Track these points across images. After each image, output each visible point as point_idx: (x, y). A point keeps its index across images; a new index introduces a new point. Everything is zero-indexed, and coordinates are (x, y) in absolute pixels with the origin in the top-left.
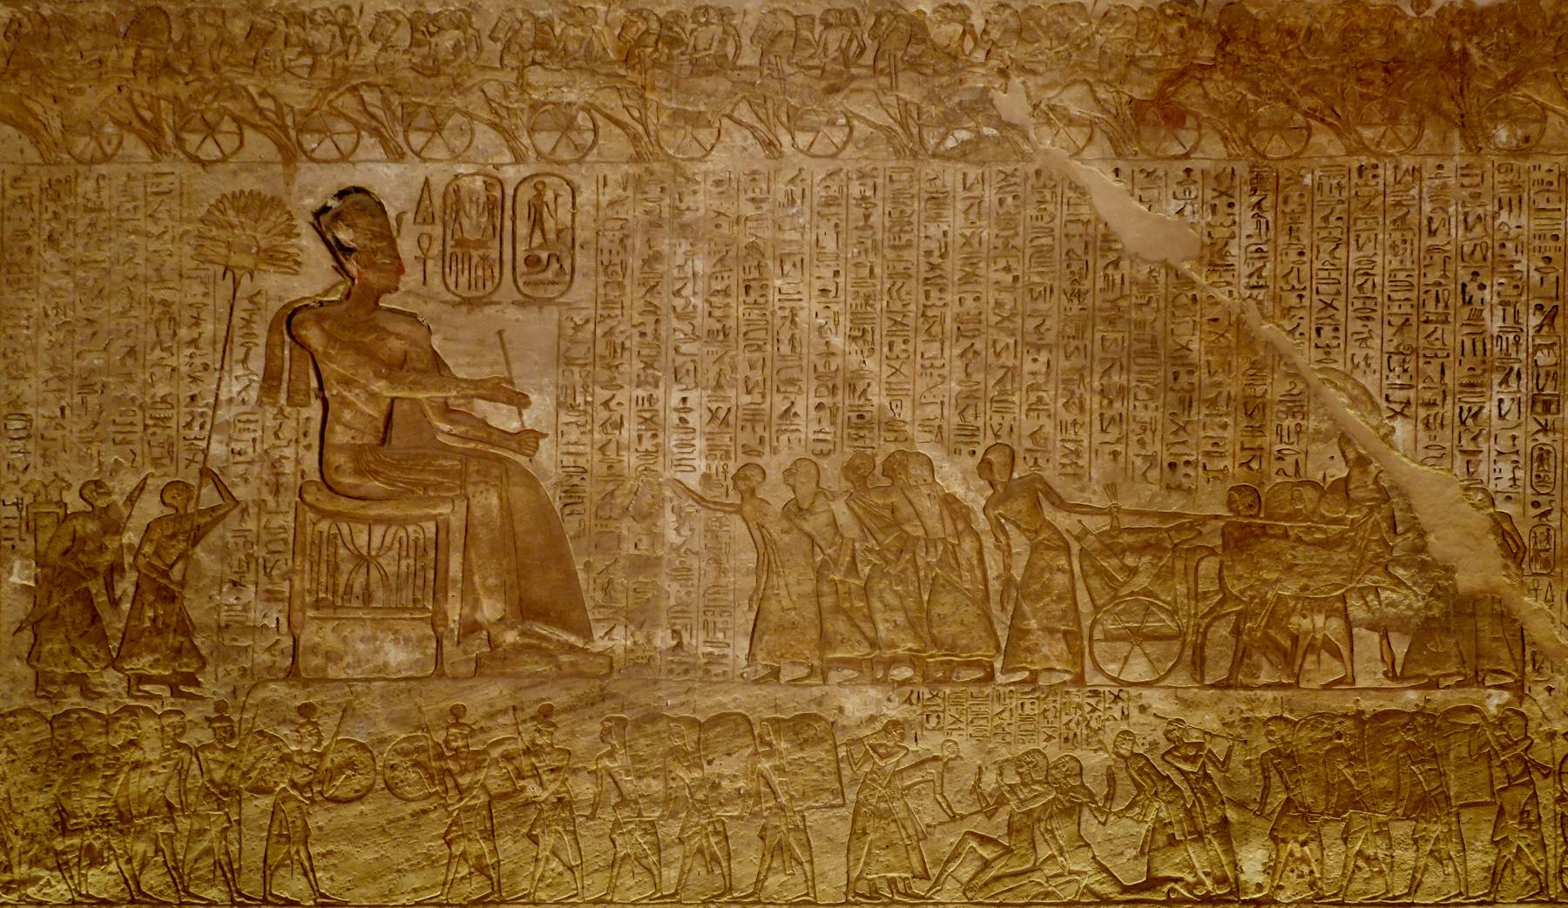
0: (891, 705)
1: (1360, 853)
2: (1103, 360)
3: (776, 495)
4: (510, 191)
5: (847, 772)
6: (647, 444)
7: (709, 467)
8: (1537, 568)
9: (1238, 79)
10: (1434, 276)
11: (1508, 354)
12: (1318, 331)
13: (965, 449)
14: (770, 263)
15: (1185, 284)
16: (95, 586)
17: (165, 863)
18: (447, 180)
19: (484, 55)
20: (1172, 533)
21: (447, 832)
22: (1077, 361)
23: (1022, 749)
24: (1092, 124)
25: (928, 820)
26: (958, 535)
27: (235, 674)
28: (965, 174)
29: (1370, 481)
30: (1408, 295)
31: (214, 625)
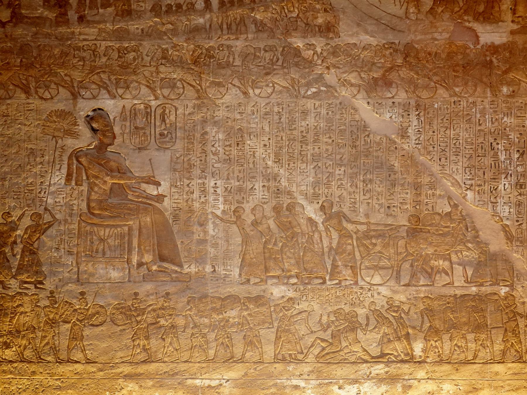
0: (289, 292)
1: (456, 344)
2: (364, 170)
3: (248, 218)
4: (153, 110)
5: (274, 316)
6: (203, 200)
7: (224, 208)
8: (518, 244)
9: (412, 70)
10: (481, 140)
11: (507, 168)
12: (440, 159)
13: (315, 201)
14: (246, 135)
15: (393, 143)
16: (7, 250)
18: (131, 106)
19: (144, 61)
20: (389, 231)
21: (132, 337)
22: (355, 170)
23: (336, 308)
24: (359, 86)
25: (303, 333)
26: (313, 232)
27: (57, 281)
28: (315, 104)
29: (458, 213)
30: (471, 147)
31: (49, 263)
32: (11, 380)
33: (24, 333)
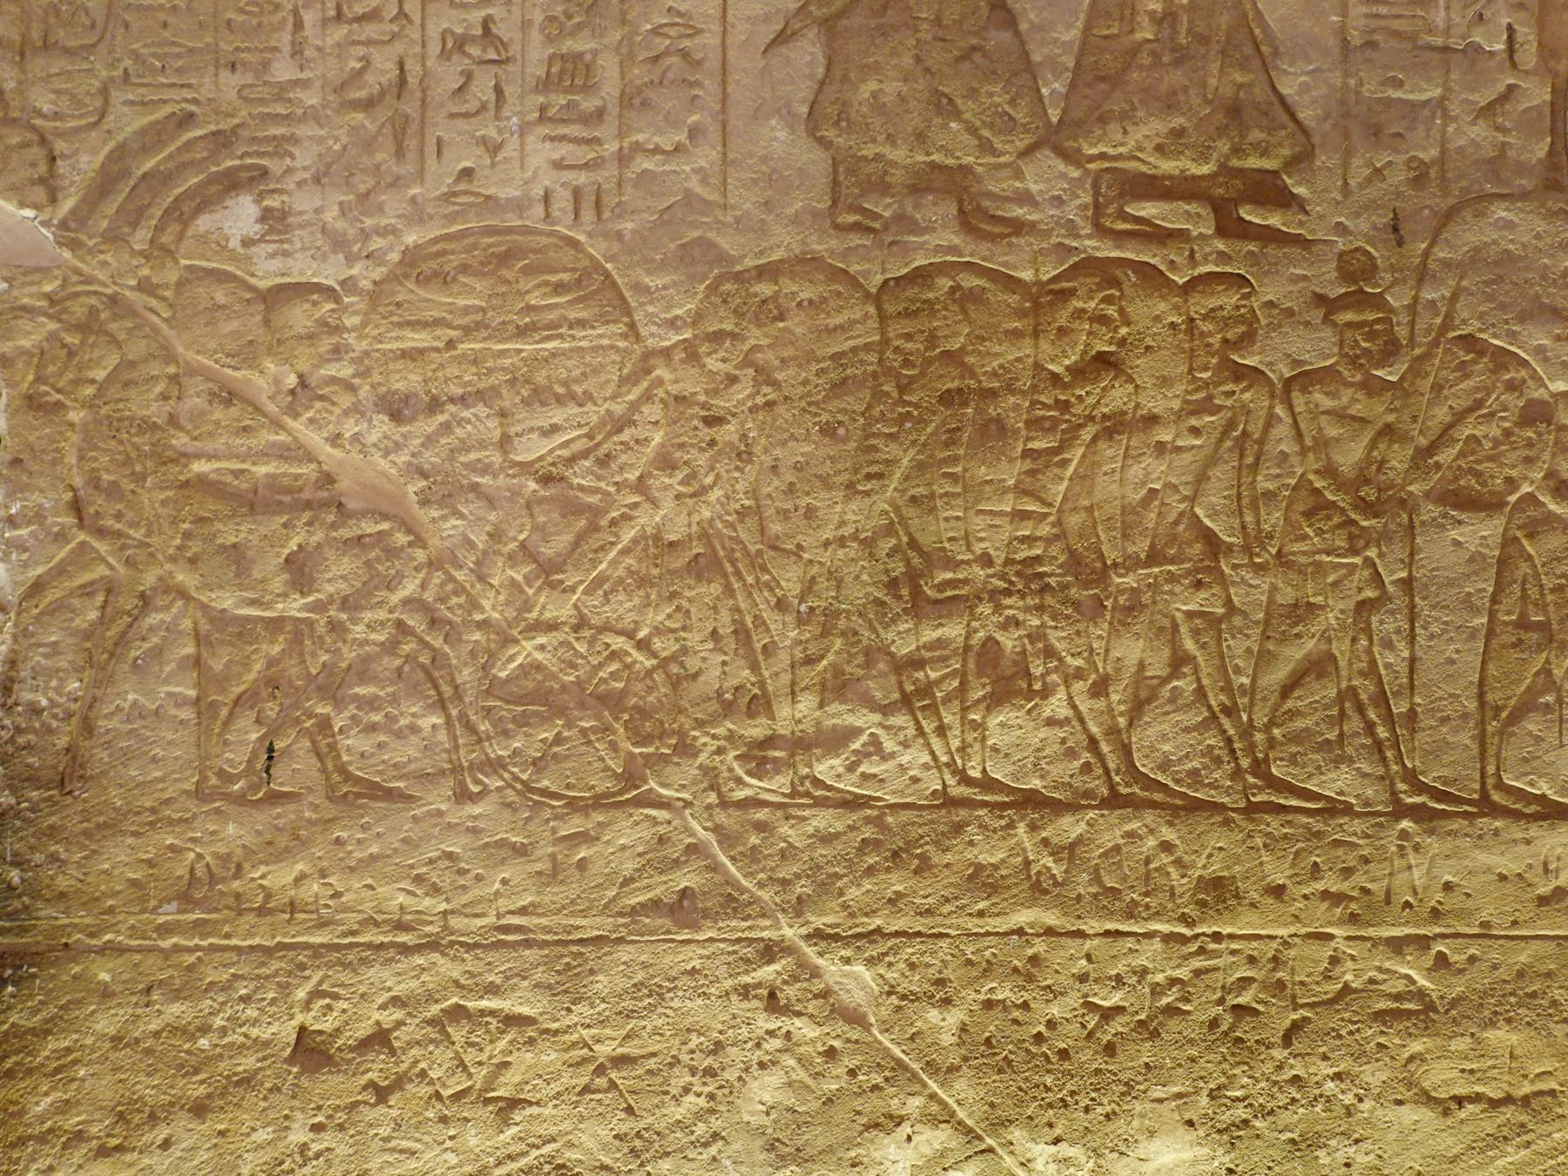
17: (1201, 693)
27: (1398, 177)
31: (1333, 42)
32: (1040, 947)
33: (1129, 581)
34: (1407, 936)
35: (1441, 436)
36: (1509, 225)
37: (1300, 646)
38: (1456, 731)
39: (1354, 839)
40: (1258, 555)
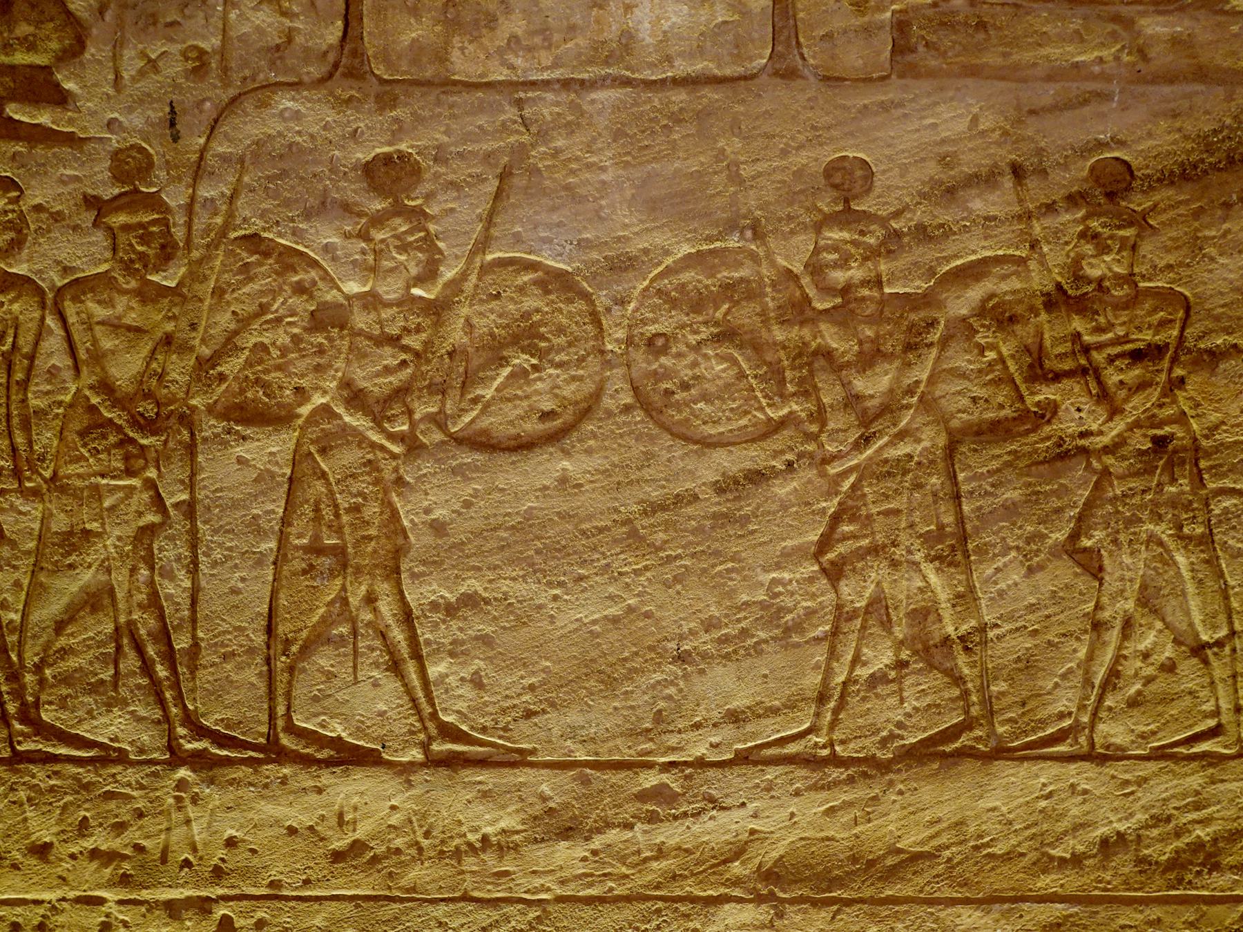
21: (825, 544)
27: (174, 68)
34: (189, 898)
35: (225, 345)
36: (297, 116)
37: (75, 578)
38: (240, 668)
39: (128, 791)
40: (29, 479)
